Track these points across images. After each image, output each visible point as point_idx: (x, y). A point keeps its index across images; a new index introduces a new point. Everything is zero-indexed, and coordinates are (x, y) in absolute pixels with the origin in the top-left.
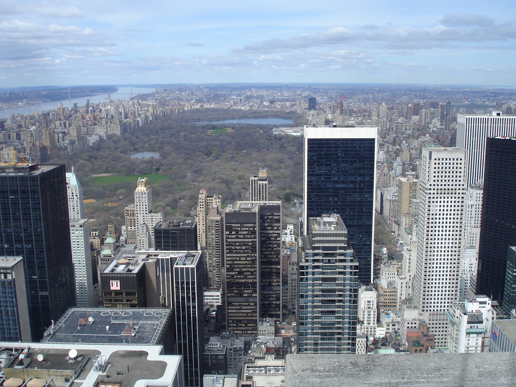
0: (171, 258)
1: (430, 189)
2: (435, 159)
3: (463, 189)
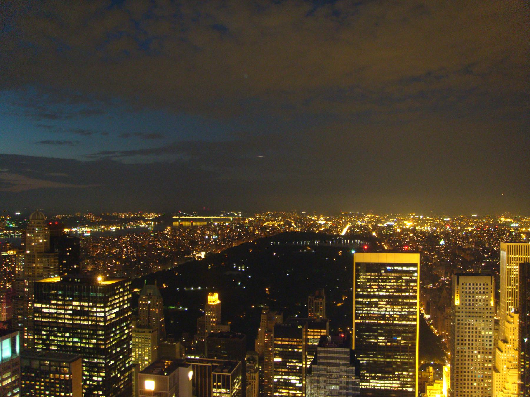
0: (213, 365)
1: (459, 312)
2: (463, 284)
3: (491, 313)
